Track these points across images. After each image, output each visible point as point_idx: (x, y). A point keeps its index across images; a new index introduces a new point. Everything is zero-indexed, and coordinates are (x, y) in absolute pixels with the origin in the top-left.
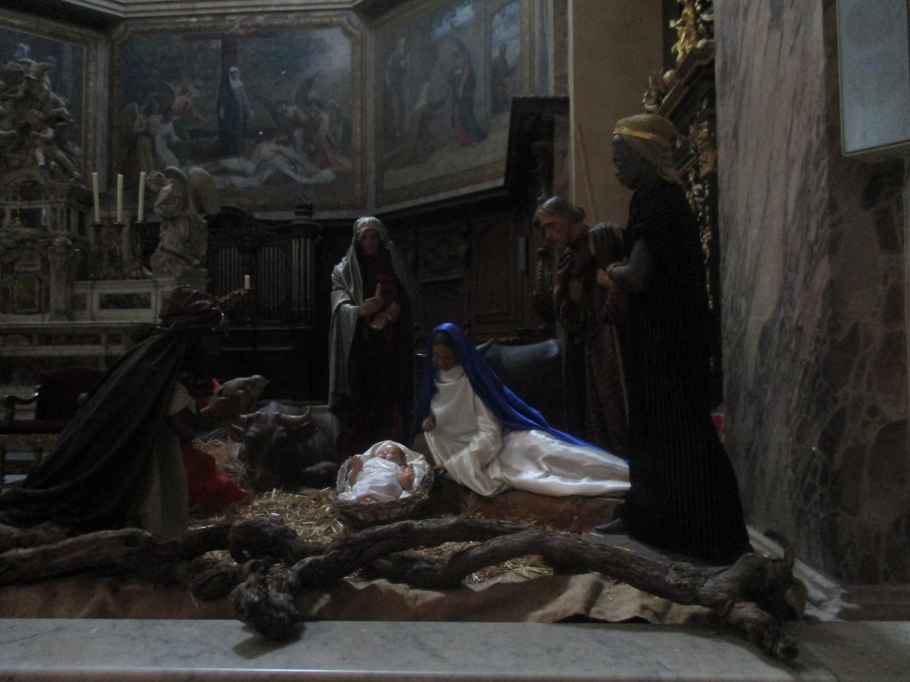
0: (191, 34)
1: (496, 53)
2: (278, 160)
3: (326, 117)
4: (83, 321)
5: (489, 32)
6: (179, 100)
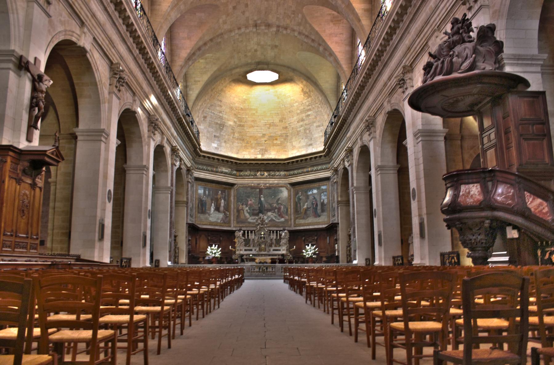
0: (252, 188)
1: (322, 201)
2: (272, 216)
3: (282, 207)
4: (271, 253)
5: (321, 196)
6: (250, 202)
